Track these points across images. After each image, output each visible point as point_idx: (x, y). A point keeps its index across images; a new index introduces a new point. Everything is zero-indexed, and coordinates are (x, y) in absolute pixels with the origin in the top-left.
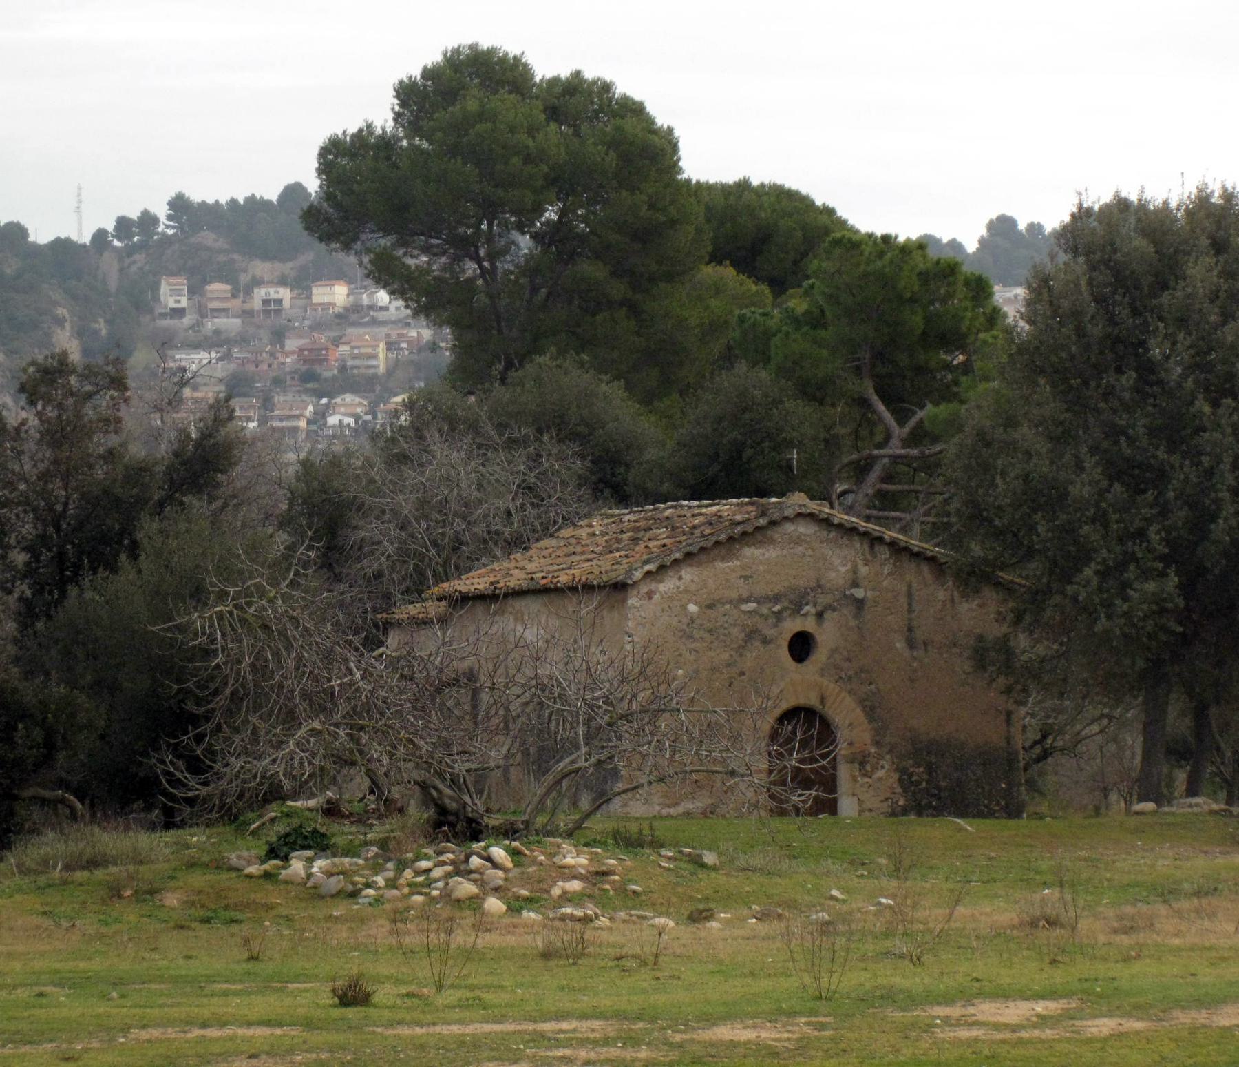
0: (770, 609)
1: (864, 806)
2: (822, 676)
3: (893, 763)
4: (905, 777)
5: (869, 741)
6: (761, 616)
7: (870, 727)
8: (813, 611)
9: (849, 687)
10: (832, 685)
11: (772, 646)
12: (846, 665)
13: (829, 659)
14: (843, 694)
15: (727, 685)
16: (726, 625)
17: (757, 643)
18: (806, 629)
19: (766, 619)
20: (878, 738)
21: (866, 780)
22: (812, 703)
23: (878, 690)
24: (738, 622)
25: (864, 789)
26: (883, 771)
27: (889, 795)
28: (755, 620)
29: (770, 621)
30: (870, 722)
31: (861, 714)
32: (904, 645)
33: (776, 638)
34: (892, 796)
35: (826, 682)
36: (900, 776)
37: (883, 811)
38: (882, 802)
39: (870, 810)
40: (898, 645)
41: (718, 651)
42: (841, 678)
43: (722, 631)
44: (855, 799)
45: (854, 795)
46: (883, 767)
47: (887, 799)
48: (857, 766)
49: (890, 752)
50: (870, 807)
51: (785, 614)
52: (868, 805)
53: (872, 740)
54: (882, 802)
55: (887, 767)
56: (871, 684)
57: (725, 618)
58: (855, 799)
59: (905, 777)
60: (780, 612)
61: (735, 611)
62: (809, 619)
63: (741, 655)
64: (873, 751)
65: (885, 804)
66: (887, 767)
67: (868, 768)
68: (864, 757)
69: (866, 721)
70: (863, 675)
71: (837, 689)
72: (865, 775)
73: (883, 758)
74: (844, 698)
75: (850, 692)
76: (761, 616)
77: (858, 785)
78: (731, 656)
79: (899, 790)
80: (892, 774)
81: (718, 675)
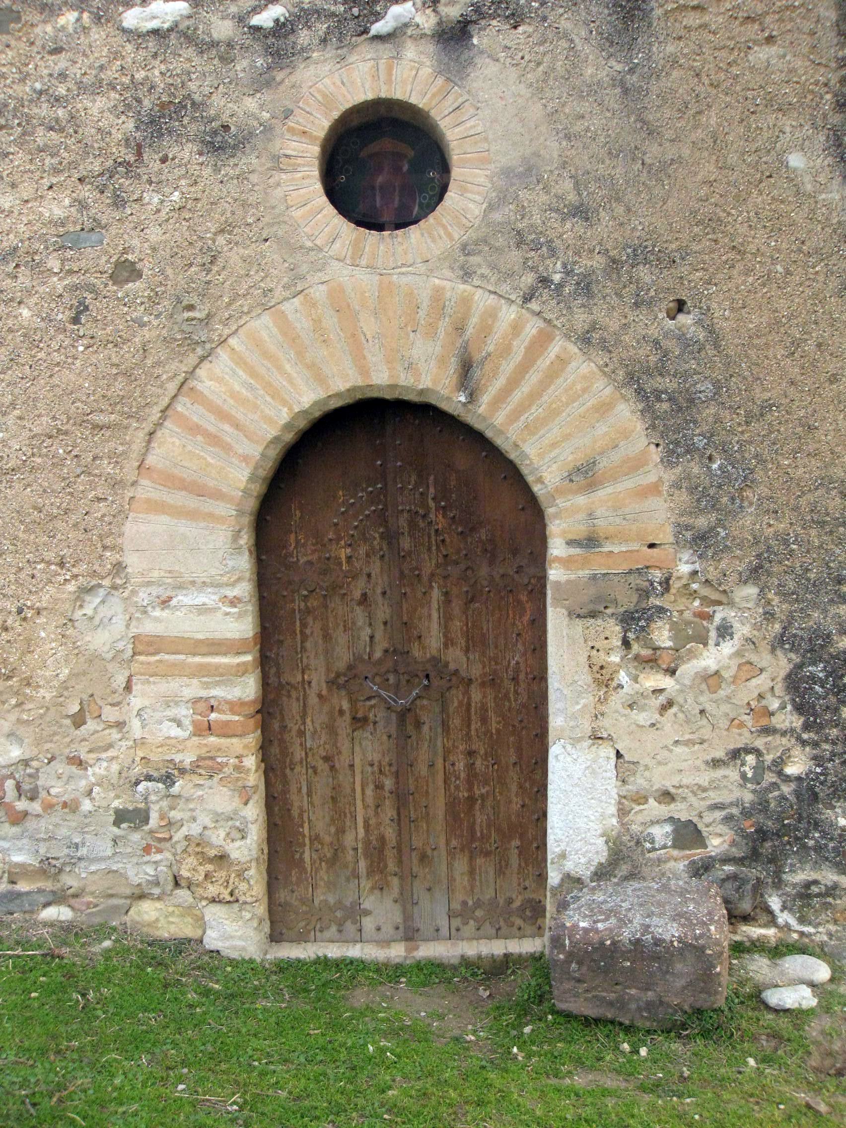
0: (241, 19)
1: (639, 782)
2: (467, 274)
3: (769, 616)
4: (818, 670)
5: (666, 536)
6: (205, 46)
7: (669, 476)
8: (427, 21)
9: (581, 319)
10: (509, 314)
11: (249, 160)
12: (571, 230)
13: (491, 208)
14: (558, 346)
15: (63, 316)
16: (62, 90)
17: (187, 152)
18: (399, 94)
19: (226, 60)
20: (702, 522)
21: (653, 680)
22: (425, 382)
23: (711, 331)
24: (109, 74)
25: (642, 718)
26: (728, 648)
27: (742, 739)
28: (177, 65)
29: (242, 65)
30: (670, 458)
31: (639, 426)
32: (823, 161)
33: (268, 129)
34: (759, 743)
35: (482, 300)
36: (799, 667)
37: (715, 797)
38: (716, 763)
39: (667, 796)
40: (796, 160)
41: (26, 190)
42: (545, 281)
43: (43, 110)
44: (606, 752)
45: (596, 738)
46: (725, 631)
47: (736, 754)
48: (615, 630)
49: (755, 573)
50: (668, 784)
51: (304, 37)
52: (660, 779)
53: (680, 528)
54: (716, 763)
55: (742, 630)
56: (681, 306)
57: (61, 62)
58: (606, 752)
59: (818, 670)
60: (281, 29)
61: (97, 35)
62: (410, 51)
63: (118, 202)
64: (684, 569)
65: (732, 774)
66: (742, 630)
67: (662, 635)
68: (645, 594)
69: (655, 454)
70: (644, 273)
71: (533, 327)
72: (651, 662)
73: (726, 599)
74: (562, 362)
75: (585, 340)
76: (205, 46)
77: (616, 701)
78: (82, 205)
79: (789, 719)
80: (764, 658)
81: (24, 279)
